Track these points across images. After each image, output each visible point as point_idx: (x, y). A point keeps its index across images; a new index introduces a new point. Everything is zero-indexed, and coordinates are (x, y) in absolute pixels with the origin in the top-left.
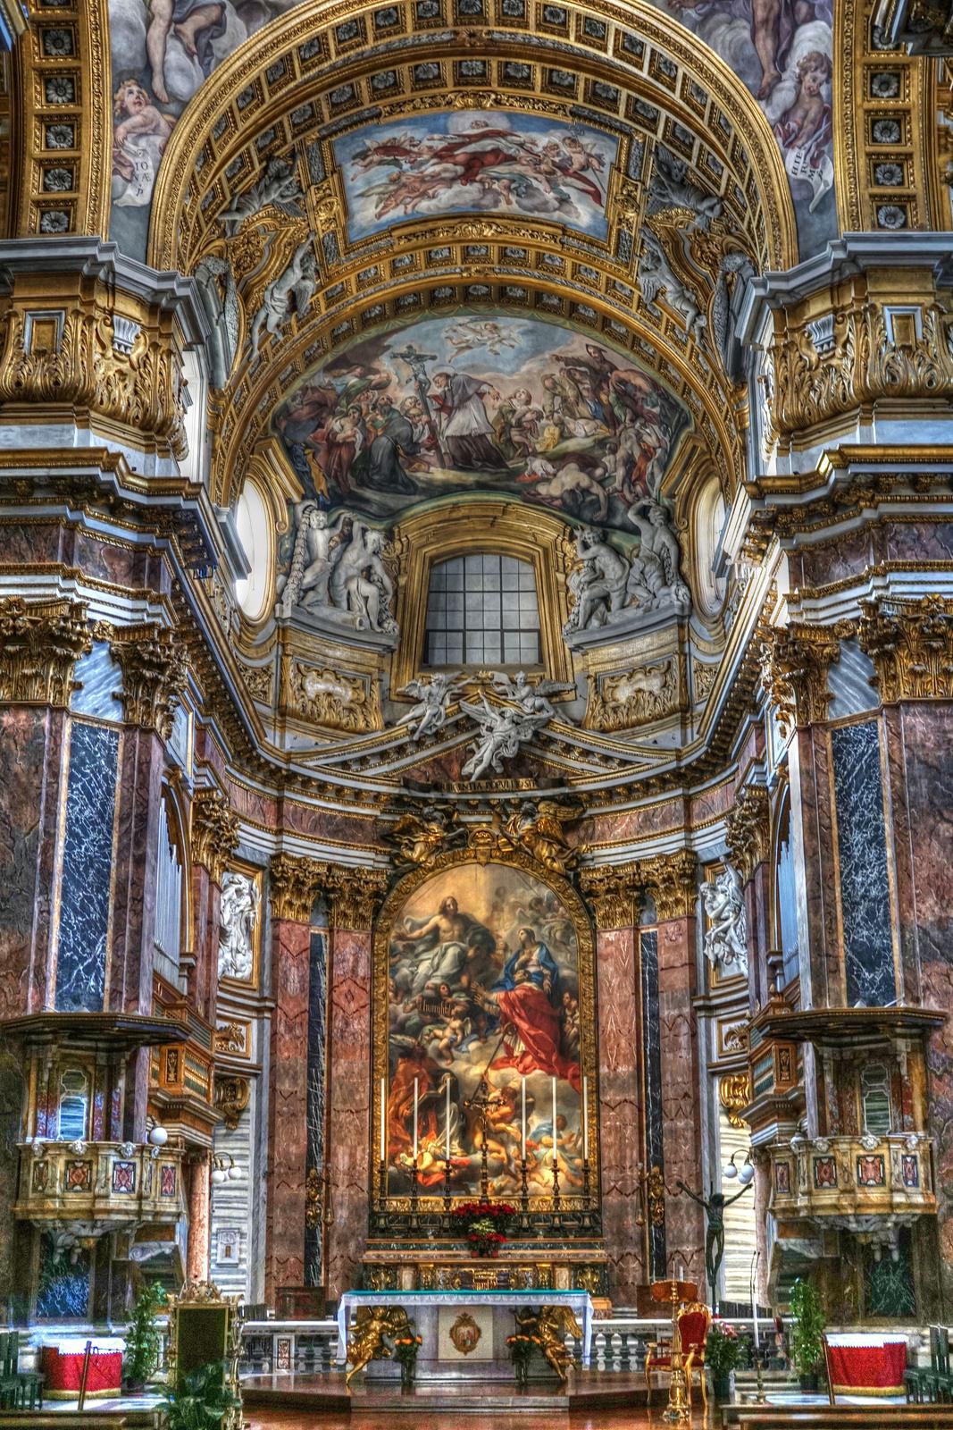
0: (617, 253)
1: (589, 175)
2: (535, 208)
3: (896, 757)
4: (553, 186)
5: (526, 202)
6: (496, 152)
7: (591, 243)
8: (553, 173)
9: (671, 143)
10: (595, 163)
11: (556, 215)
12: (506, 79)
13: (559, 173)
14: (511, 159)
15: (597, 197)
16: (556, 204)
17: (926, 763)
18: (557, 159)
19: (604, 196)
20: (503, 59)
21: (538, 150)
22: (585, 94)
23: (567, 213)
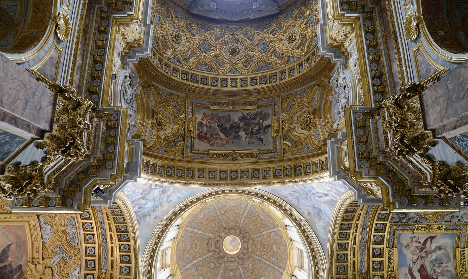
0: (460, 230)
1: (422, 241)
2: (448, 257)
3: (453, 125)
4: (434, 251)
5: (445, 260)
6: (419, 271)
7: (459, 238)
8: (426, 253)
9: (388, 218)
10: (414, 239)
11: (449, 250)
12: (381, 269)
13: (425, 250)
14: (422, 266)
15: (432, 238)
16: (442, 251)
17: (447, 108)
18: (418, 251)
19: (430, 235)
20: (371, 270)
21: (415, 257)
22: (380, 245)
23: (446, 247)
